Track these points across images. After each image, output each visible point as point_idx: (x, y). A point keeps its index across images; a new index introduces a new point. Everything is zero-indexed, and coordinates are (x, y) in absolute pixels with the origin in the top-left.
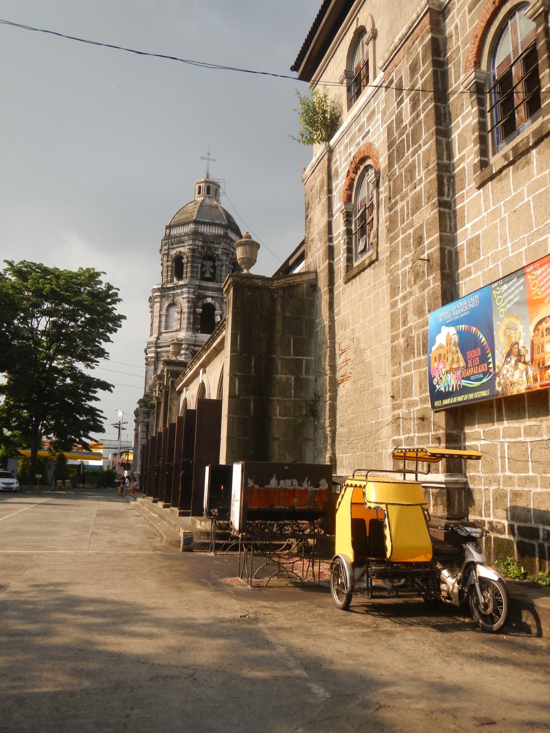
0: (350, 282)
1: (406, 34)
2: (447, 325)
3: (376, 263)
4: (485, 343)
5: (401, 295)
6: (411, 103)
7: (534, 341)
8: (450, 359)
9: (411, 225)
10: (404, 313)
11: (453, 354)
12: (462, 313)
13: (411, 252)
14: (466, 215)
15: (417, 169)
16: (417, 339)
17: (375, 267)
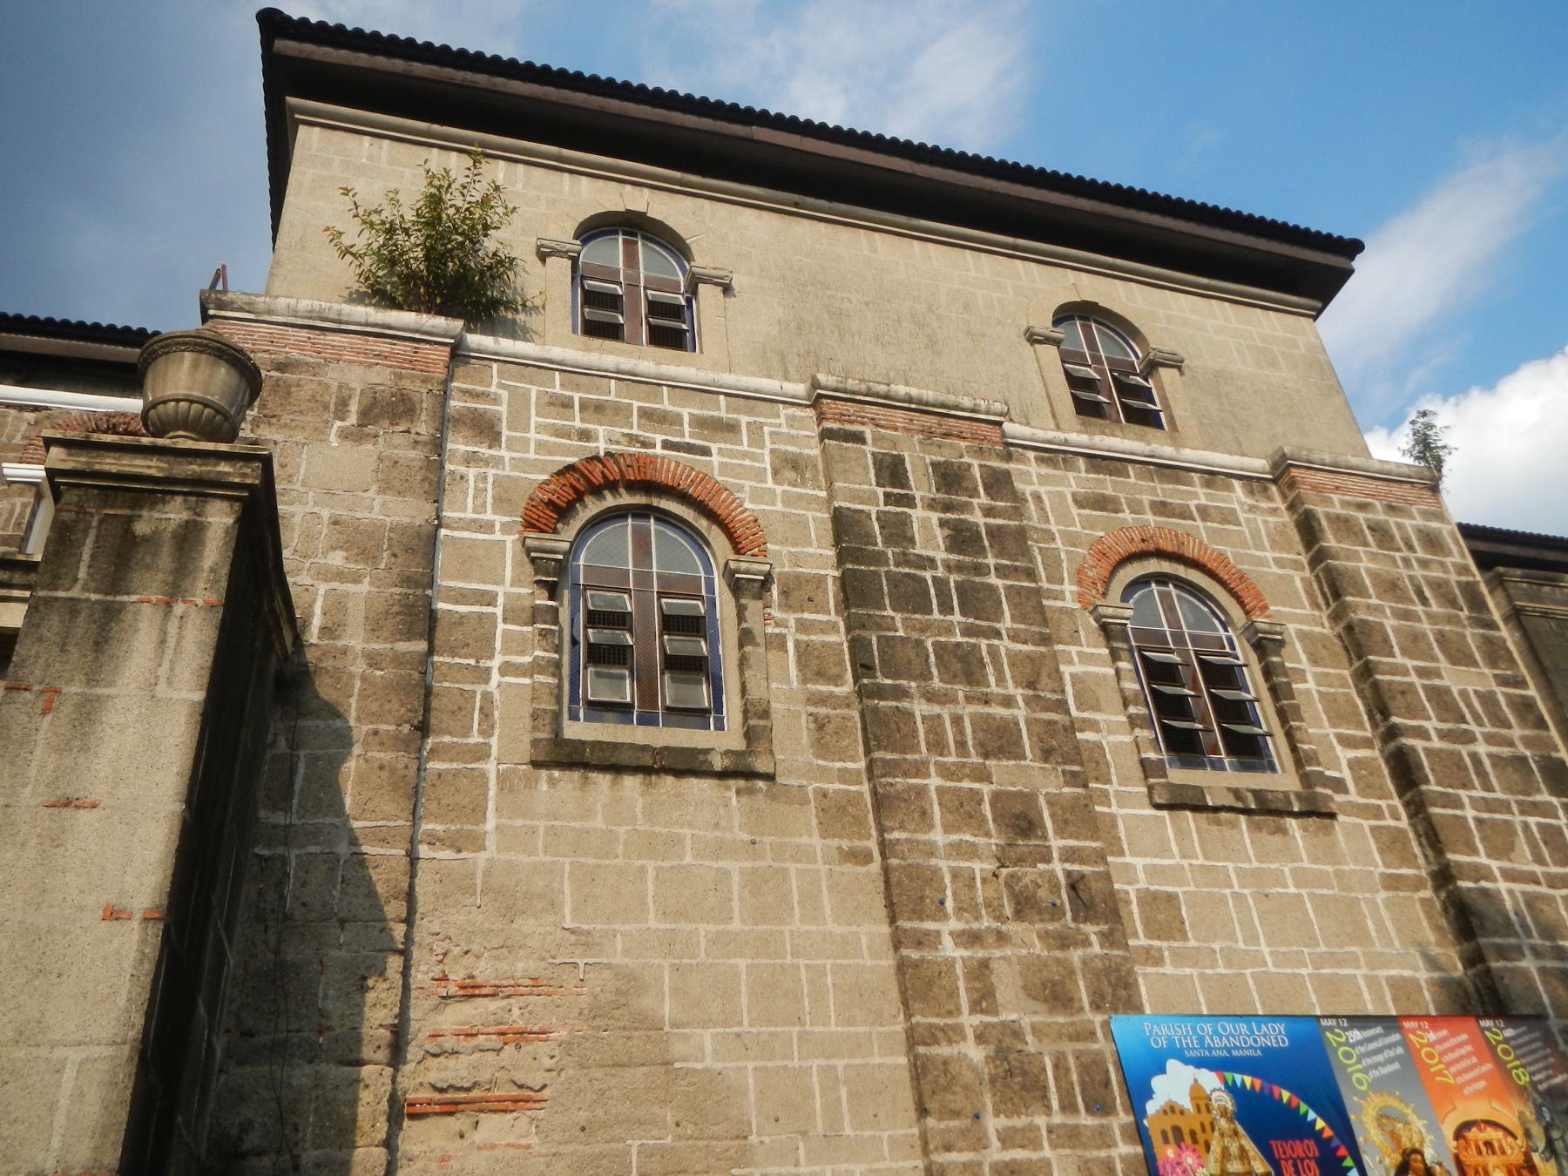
0: (576, 775)
1: (927, 404)
2: (1200, 1063)
3: (761, 784)
4: (1328, 1133)
5: (954, 924)
6: (947, 532)
7: (1462, 1158)
8: (1215, 1146)
9: (985, 777)
10: (977, 978)
11: (1222, 1135)
12: (1236, 1048)
13: (988, 834)
14: (1123, 837)
15: (990, 670)
16: (1056, 1067)
17: (751, 792)
